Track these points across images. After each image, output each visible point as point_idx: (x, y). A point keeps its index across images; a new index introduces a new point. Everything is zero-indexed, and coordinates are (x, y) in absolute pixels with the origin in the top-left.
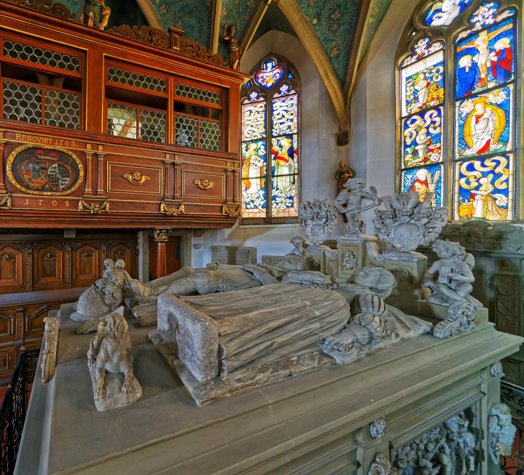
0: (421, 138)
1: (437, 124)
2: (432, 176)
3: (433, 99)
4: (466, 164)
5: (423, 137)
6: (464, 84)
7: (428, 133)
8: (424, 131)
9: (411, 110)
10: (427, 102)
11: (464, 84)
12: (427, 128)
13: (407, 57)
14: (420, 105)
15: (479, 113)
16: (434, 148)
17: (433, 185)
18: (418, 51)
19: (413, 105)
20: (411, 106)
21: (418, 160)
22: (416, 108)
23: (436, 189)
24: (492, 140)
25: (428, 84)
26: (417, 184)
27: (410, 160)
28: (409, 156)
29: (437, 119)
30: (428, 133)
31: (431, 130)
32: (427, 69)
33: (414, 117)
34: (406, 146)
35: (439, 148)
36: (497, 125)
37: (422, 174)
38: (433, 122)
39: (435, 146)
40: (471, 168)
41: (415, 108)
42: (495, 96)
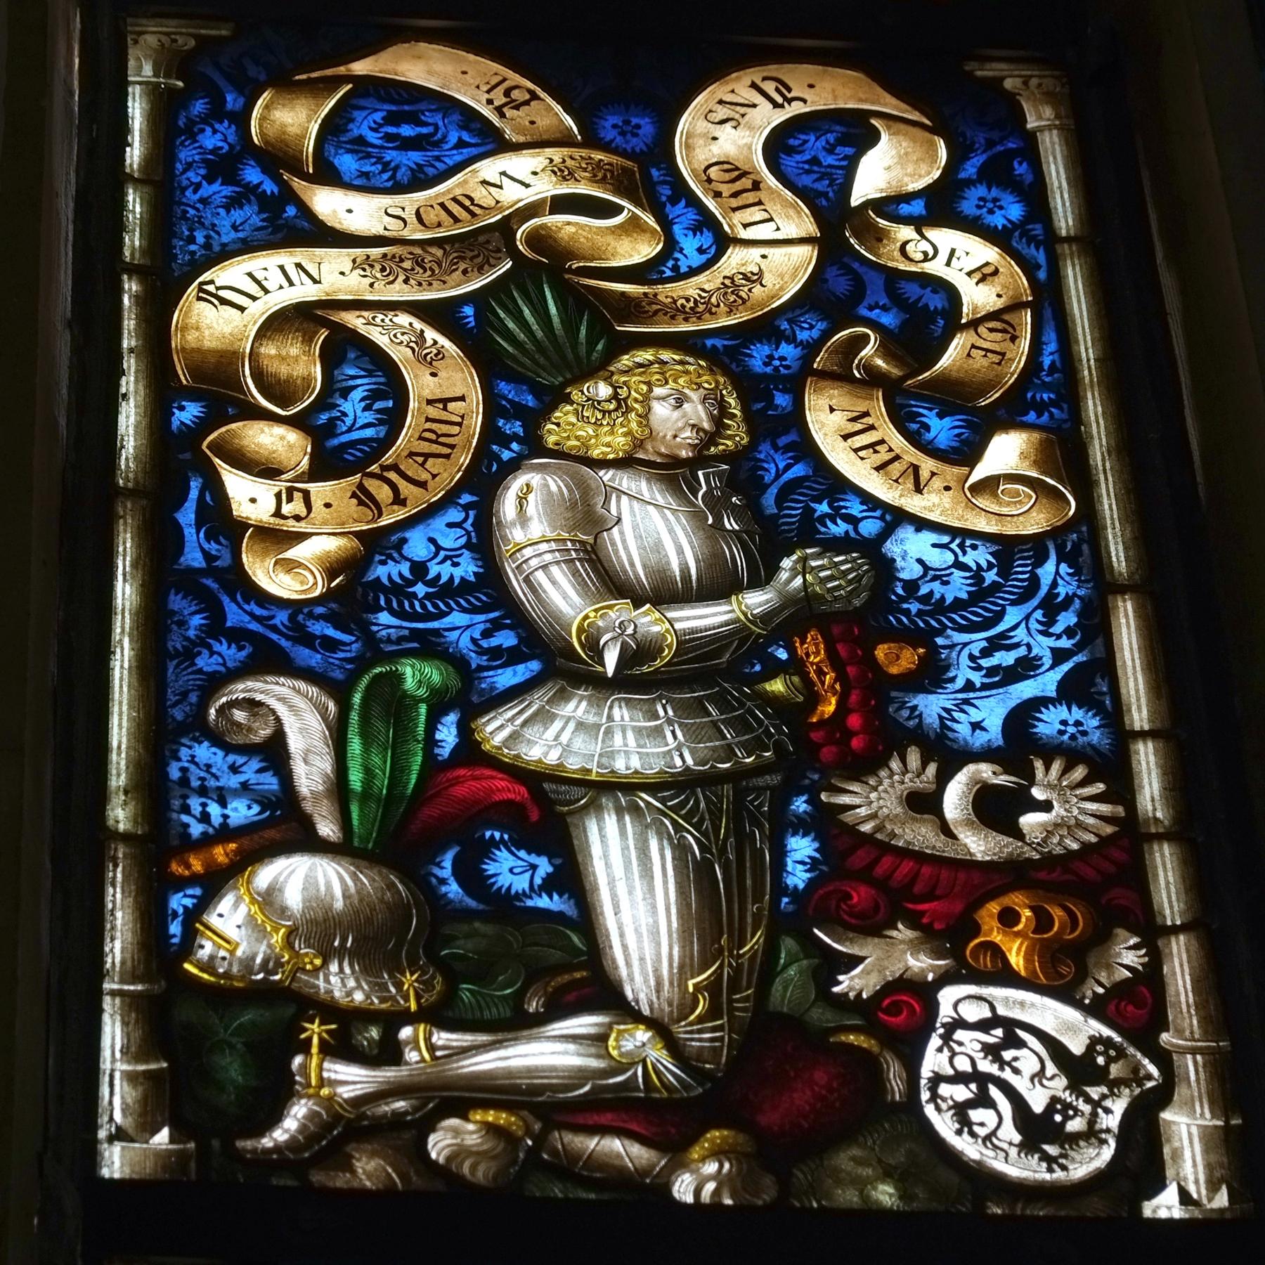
0: (612, 525)
5: (654, 529)
7: (759, 488)
12: (759, 367)
16: (978, 845)
21: (549, 1051)
27: (341, 983)
29: (961, 260)
35: (1097, 887)
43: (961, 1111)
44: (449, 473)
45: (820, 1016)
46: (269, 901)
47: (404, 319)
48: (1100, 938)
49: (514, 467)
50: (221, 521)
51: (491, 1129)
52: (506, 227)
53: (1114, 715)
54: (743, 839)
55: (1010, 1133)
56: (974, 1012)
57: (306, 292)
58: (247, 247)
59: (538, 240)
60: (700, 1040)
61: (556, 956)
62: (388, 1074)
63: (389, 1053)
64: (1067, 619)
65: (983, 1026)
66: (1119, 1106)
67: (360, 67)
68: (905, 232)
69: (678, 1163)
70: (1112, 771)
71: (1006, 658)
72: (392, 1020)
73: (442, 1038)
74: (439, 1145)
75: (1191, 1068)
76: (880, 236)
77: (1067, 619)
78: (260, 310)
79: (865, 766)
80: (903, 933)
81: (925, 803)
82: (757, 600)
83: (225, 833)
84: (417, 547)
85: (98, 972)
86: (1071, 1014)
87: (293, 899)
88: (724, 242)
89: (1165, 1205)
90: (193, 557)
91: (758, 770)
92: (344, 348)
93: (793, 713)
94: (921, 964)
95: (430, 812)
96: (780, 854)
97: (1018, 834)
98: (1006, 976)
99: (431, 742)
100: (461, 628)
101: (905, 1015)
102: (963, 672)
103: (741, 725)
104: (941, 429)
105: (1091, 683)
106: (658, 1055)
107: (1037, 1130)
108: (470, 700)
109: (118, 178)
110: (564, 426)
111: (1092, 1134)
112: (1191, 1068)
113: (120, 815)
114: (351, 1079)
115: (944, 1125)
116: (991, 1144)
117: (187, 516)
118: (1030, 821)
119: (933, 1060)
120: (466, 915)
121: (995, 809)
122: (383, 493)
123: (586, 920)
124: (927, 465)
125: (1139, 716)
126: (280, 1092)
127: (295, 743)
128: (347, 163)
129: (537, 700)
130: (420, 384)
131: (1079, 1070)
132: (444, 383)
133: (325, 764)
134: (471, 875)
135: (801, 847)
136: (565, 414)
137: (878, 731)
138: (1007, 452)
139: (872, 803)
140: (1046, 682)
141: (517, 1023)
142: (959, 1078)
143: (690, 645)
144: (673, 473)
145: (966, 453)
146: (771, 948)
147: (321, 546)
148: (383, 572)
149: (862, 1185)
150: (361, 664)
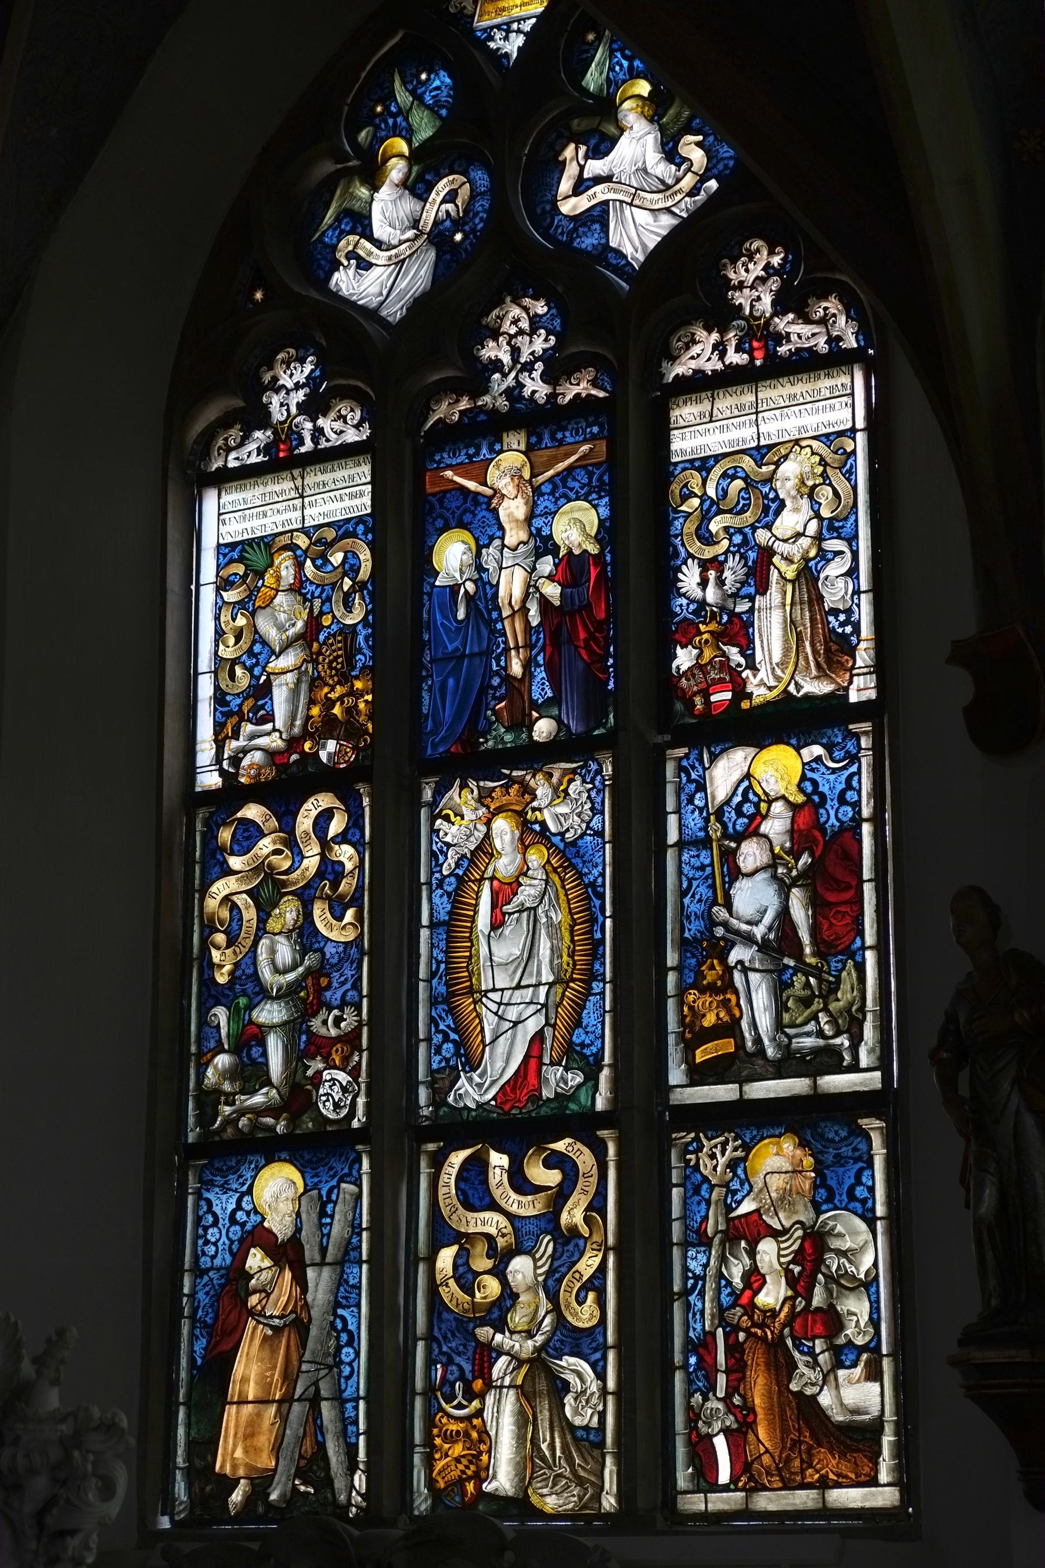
1: (347, 886)
2: (323, 1214)
3: (329, 727)
4: (458, 1158)
5: (285, 953)
6: (451, 682)
7: (305, 935)
8: (288, 912)
9: (235, 761)
10: (305, 735)
11: (451, 682)
13: (225, 423)
14: (274, 742)
15: (505, 865)
16: (333, 1032)
17: (326, 1272)
18: (276, 406)
19: (248, 728)
20: (236, 735)
21: (258, 1099)
22: (257, 756)
23: (337, 1304)
24: (548, 1032)
25: (314, 624)
26: (256, 1259)
27: (227, 1087)
28: (223, 1060)
29: (345, 854)
30: (305, 935)
31: (320, 912)
32: (304, 530)
33: (253, 812)
34: (213, 994)
35: (351, 1039)
36: (565, 958)
37: (277, 1190)
38: (330, 870)
39: (338, 1021)
40: (475, 1191)
41: (261, 743)
42: (555, 790)
43: (324, 1102)
44: (249, 943)
45: (304, 1082)
46: (216, 1067)
47: (244, 896)
48: (352, 1054)
49: (261, 938)
50: (212, 965)
51: (249, 1119)
52: (263, 862)
53: (360, 992)
54: (293, 1036)
55: (332, 1108)
56: (328, 1078)
57: (227, 892)
58: (218, 879)
59: (270, 866)
60: (283, 1091)
61: (261, 1073)
62: (233, 1108)
63: (233, 1104)
64: (355, 965)
65: (329, 1081)
66: (350, 1098)
67: (239, 815)
68: (336, 847)
69: (277, 1123)
70: (358, 1008)
71: (342, 979)
72: (235, 1094)
73: (243, 1097)
74: (241, 1124)
75: (363, 1086)
76: (331, 849)
77: (355, 965)
78: (219, 898)
79: (315, 1014)
80: (319, 1058)
81: (325, 1022)
82: (301, 969)
83: (210, 1051)
84: (243, 967)
85: (188, 1091)
86: (344, 1075)
87: (220, 1066)
88: (303, 857)
89: (355, 1124)
90: (206, 976)
91: (298, 1018)
92: (234, 907)
93: (304, 1001)
94: (321, 1066)
95: (245, 1037)
96: (300, 1040)
97: (340, 1028)
98: (335, 1067)
99: (244, 1020)
100: (250, 986)
101: (317, 1080)
102: (335, 984)
103: (295, 1006)
104: (338, 910)
105: (357, 985)
106: (277, 1096)
107: (337, 1106)
108: (250, 1007)
109: (194, 862)
110: (273, 925)
111: (345, 1106)
112: (363, 1086)
113: (193, 1049)
114: (228, 1110)
115: (321, 1106)
116: (327, 1110)
117: (205, 964)
118: (343, 1025)
119: (321, 1091)
120: (248, 1065)
121: (338, 1021)
122: (238, 951)
123: (266, 1064)
124: (334, 922)
125: (365, 992)
126: (216, 1114)
127: (222, 1025)
128: (236, 848)
129: (263, 1003)
130: (246, 916)
131: (344, 1090)
132: (250, 914)
133: (226, 1029)
134: (249, 1055)
135: (304, 1038)
136: (270, 921)
137: (320, 1004)
138: (350, 915)
139: (316, 1024)
140: (348, 986)
141: (253, 1092)
142: (324, 1095)
143: (290, 985)
144: (288, 934)
145: (340, 919)
146: (297, 1065)
147: (228, 968)
148: (238, 973)
149: (307, 1123)
150: (233, 1000)
